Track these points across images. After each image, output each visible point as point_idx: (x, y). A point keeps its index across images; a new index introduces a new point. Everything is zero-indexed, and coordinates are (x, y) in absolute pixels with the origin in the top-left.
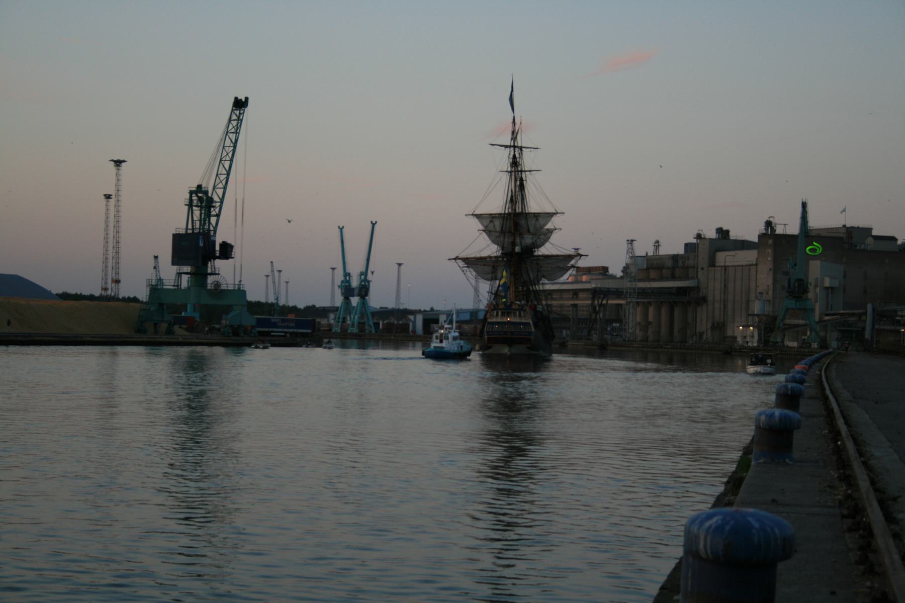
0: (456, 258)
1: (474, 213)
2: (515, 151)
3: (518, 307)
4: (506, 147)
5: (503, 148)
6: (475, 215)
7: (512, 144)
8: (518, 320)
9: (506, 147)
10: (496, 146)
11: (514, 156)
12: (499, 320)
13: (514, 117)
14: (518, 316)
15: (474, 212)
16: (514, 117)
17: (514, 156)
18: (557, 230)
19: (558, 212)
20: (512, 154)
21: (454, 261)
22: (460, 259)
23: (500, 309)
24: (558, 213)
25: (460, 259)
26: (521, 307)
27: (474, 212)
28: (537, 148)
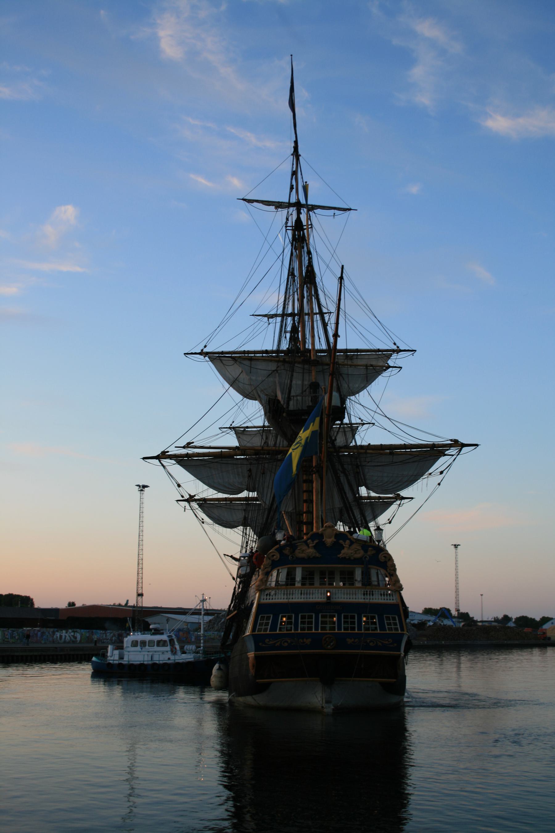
0: (163, 456)
1: (206, 350)
2: (299, 213)
3: (360, 554)
4: (279, 205)
5: (272, 208)
6: (206, 354)
7: (293, 200)
8: (358, 597)
9: (279, 205)
10: (255, 204)
11: (298, 220)
12: (297, 597)
13: (296, 142)
14: (358, 584)
15: (205, 346)
16: (296, 142)
17: (298, 220)
18: (366, 426)
19: (402, 348)
20: (295, 217)
21: (156, 461)
22: (171, 457)
23: (301, 561)
24: (398, 351)
25: (171, 457)
26: (371, 552)
27: (205, 346)
28: (350, 209)
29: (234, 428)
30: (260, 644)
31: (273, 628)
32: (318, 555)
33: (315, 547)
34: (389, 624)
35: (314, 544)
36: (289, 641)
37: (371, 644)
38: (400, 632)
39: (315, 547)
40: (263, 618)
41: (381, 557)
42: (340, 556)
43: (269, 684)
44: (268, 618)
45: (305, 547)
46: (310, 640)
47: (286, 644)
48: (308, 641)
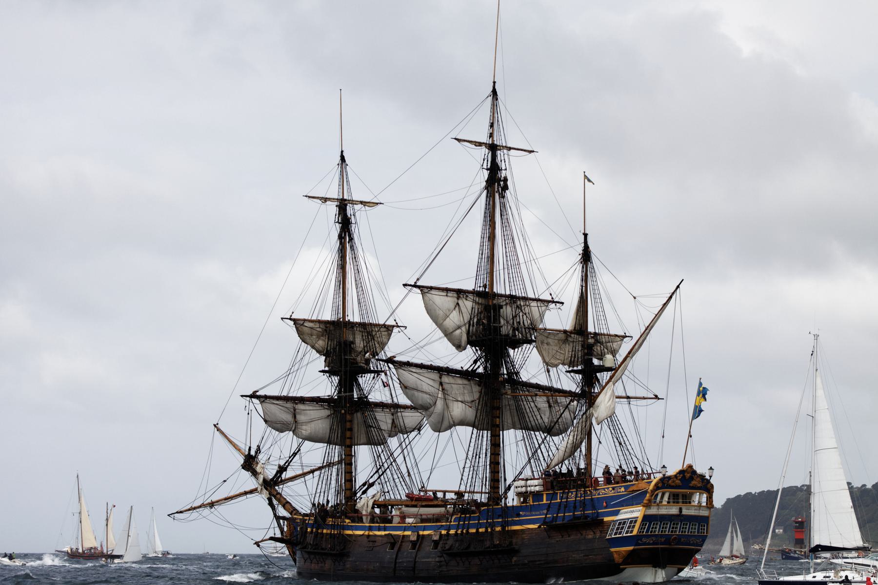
12: (663, 511)
29: (295, 321)
30: (639, 541)
31: (647, 531)
32: (681, 484)
33: (680, 480)
34: (701, 529)
35: (680, 478)
36: (654, 539)
37: (692, 542)
38: (705, 534)
39: (680, 480)
40: (674, 524)
41: (709, 486)
42: (691, 485)
43: (624, 569)
44: (646, 524)
45: (675, 479)
46: (664, 539)
47: (652, 541)
48: (663, 540)
